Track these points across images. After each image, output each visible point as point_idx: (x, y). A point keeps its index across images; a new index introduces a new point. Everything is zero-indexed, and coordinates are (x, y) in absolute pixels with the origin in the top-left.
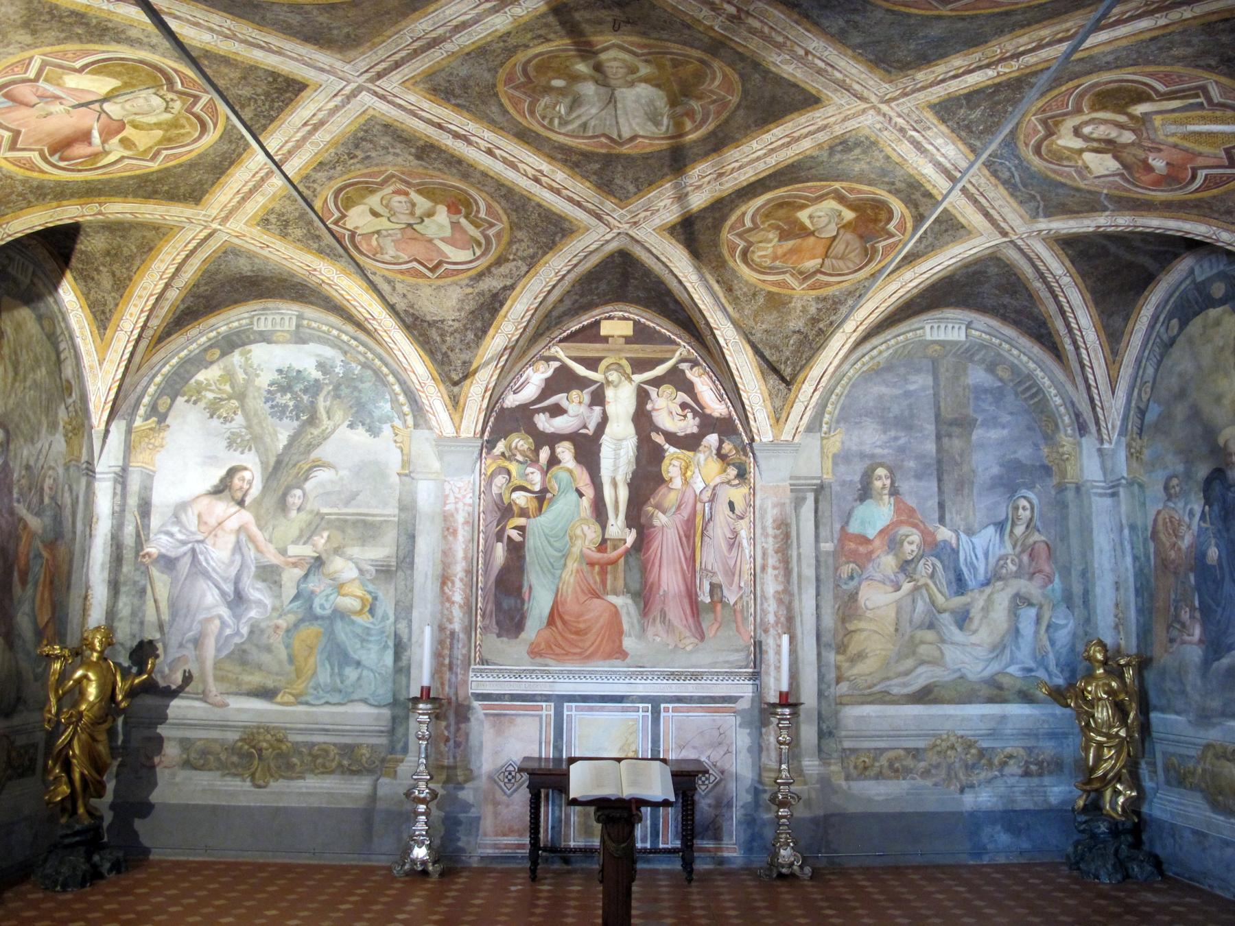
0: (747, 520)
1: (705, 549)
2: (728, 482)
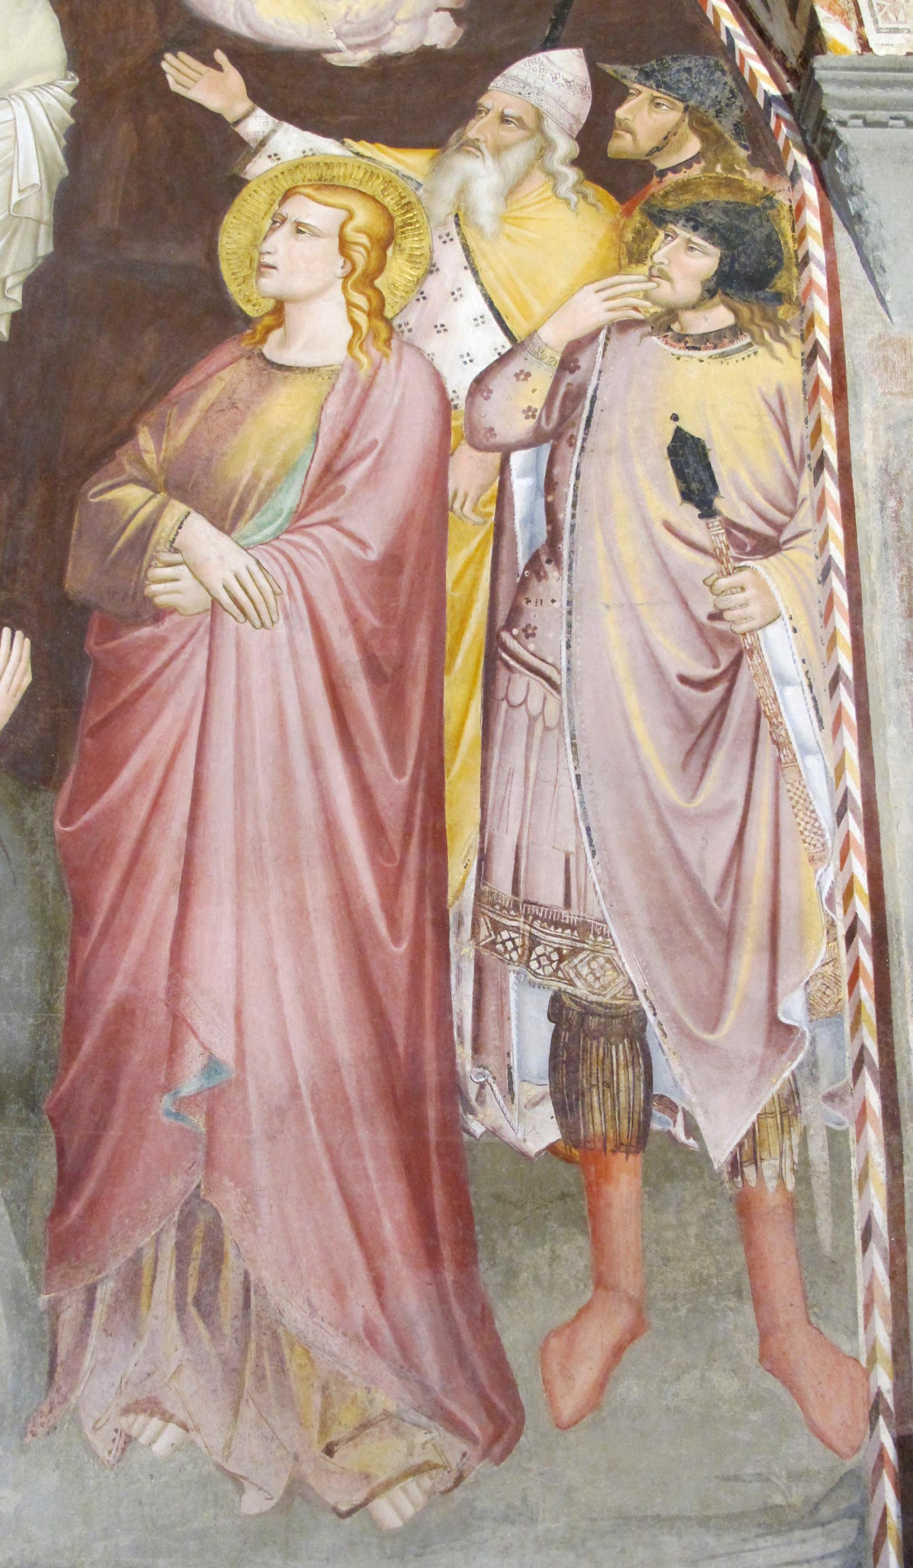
0: (800, 557)
1: (512, 756)
2: (665, 322)
